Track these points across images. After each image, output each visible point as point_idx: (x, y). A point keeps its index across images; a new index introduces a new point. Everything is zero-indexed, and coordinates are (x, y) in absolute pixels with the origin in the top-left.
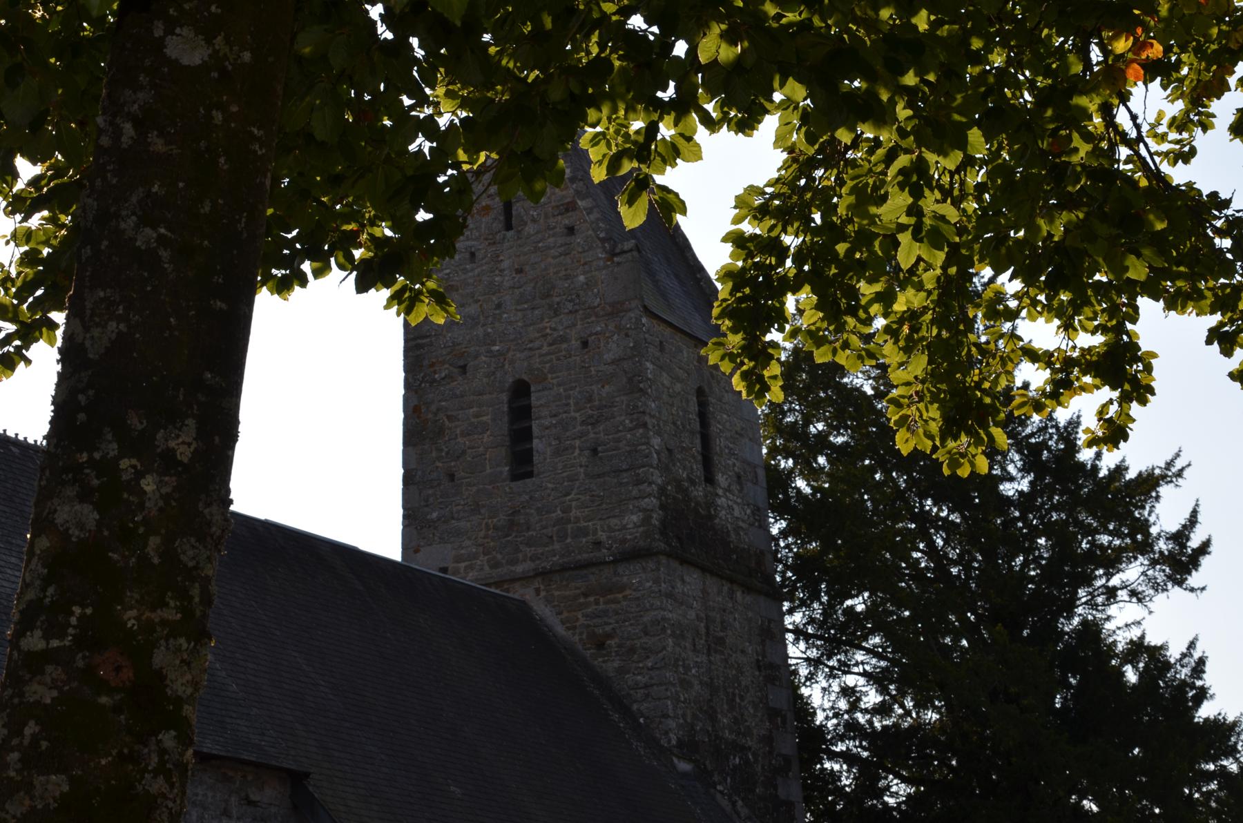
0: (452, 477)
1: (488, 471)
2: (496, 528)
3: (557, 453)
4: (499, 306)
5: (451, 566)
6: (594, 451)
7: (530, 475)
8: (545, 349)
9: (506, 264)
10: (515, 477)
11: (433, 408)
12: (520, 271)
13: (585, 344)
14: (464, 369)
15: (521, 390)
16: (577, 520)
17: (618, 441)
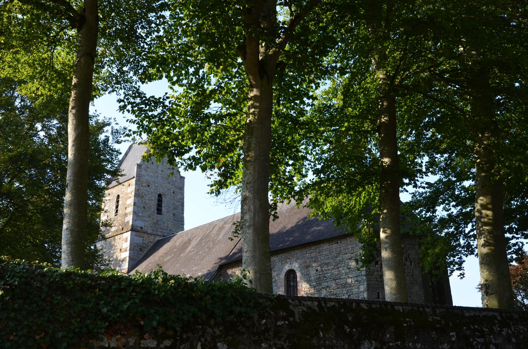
0: (144, 208)
1: (152, 210)
2: (153, 223)
3: (167, 212)
4: (157, 176)
5: (143, 227)
6: (174, 215)
7: (161, 214)
8: (166, 190)
9: (159, 168)
10: (157, 214)
11: (142, 191)
12: (162, 171)
13: (174, 192)
14: (148, 186)
15: (160, 196)
16: (170, 227)
17: (179, 215)
